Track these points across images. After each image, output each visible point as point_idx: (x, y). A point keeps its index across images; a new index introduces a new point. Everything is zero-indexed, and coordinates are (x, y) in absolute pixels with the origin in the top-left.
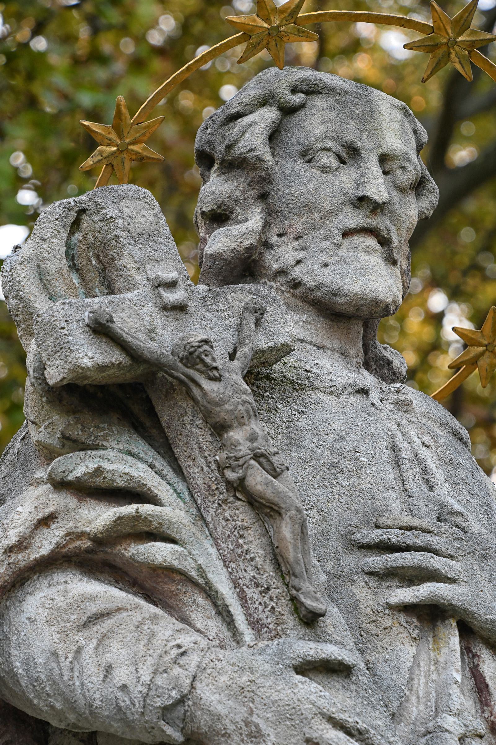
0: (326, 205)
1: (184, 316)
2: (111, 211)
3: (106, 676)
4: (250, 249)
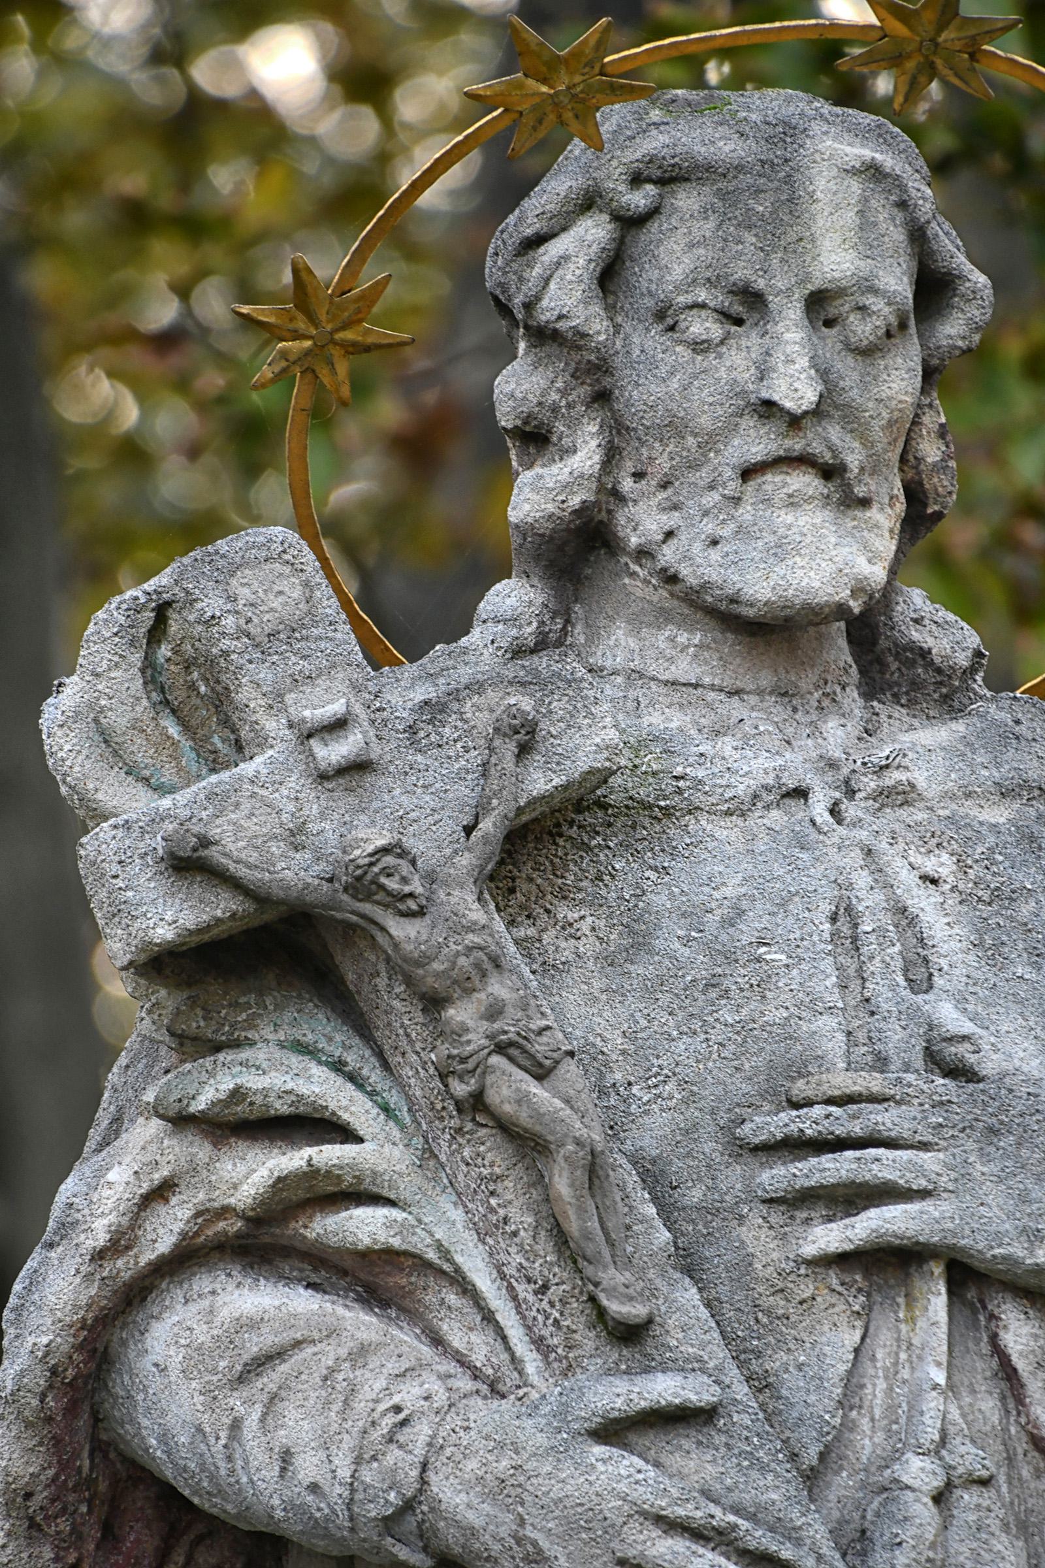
0: (705, 421)
1: (369, 779)
2: (212, 604)
3: (283, 1470)
4: (583, 510)
